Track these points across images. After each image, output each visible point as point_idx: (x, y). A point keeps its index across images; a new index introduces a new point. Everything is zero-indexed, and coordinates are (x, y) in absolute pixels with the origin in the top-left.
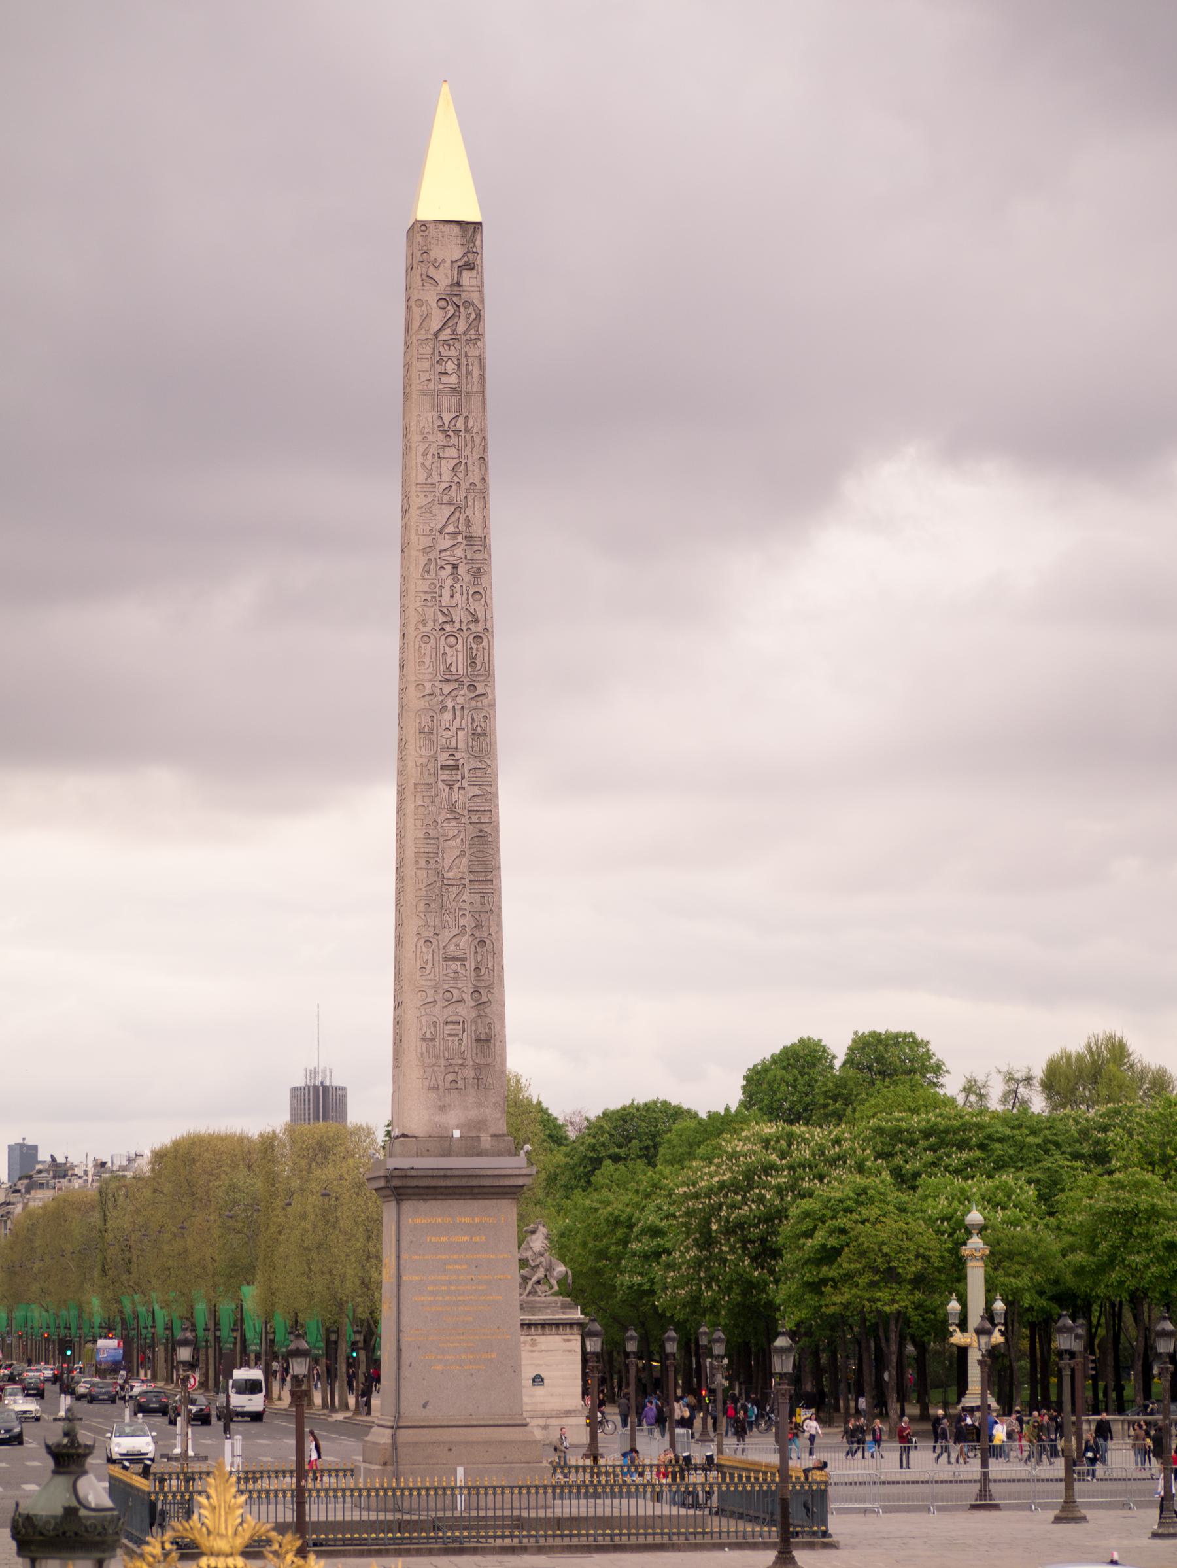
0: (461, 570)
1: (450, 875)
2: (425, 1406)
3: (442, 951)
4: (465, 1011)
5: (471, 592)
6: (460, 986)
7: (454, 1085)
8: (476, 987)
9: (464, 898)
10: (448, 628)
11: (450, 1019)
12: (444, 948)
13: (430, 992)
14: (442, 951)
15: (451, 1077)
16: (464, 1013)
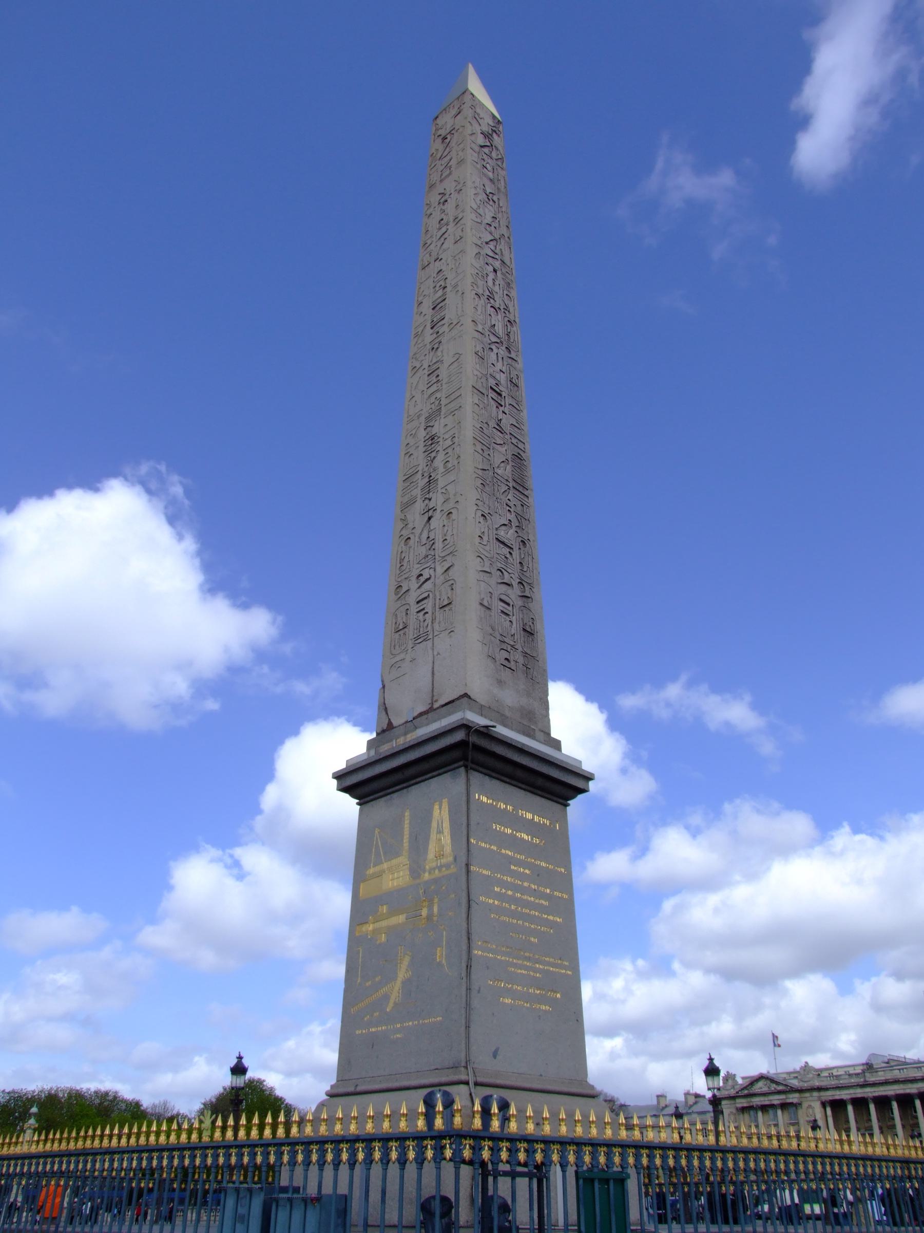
0: (499, 273)
1: (499, 472)
2: (495, 1055)
3: (495, 532)
4: (513, 594)
5: (505, 292)
6: (510, 571)
7: (506, 663)
8: (521, 579)
9: (509, 497)
10: (492, 301)
11: (504, 597)
12: (497, 529)
13: (487, 563)
14: (495, 532)
15: (506, 655)
16: (513, 597)
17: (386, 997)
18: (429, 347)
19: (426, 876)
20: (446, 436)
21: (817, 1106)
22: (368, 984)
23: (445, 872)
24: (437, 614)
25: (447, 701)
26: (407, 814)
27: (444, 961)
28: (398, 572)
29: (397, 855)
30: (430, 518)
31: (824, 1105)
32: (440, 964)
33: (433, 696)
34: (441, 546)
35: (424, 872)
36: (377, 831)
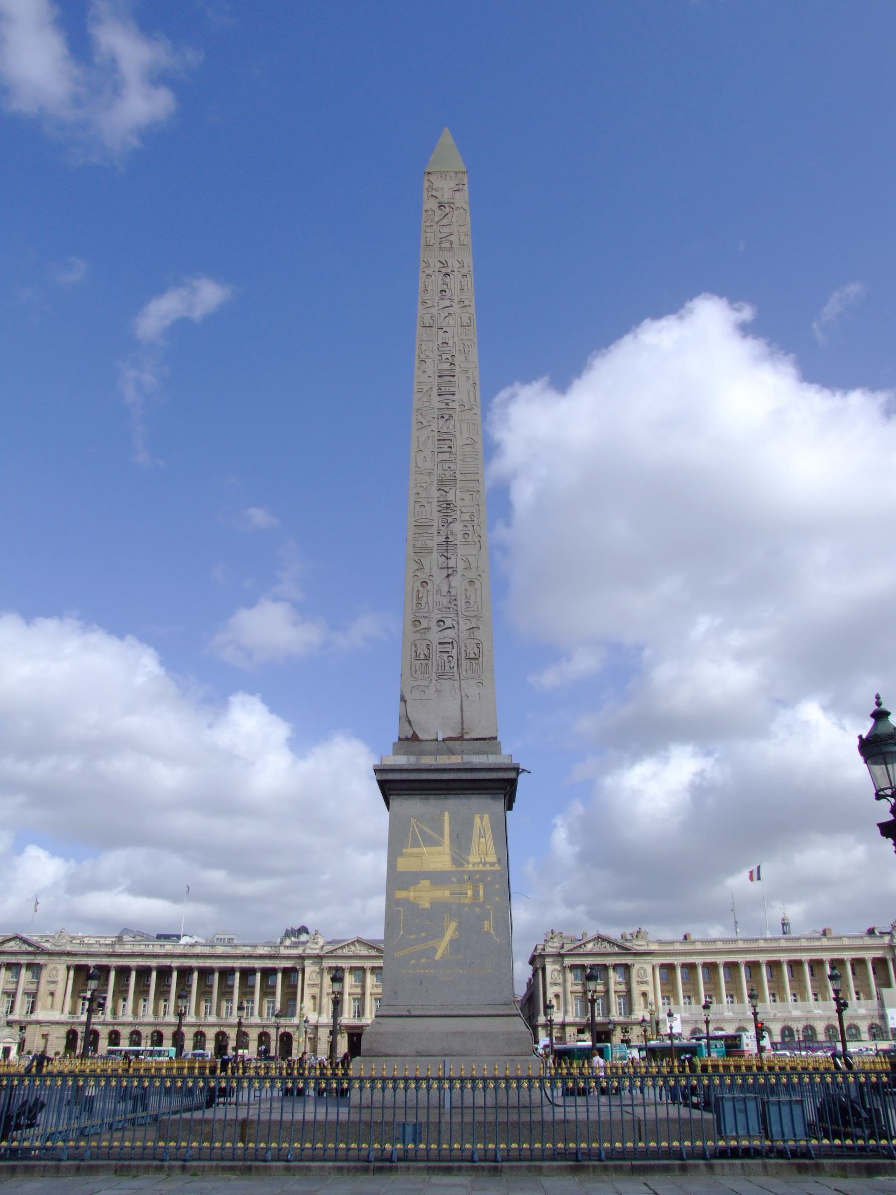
17: (435, 950)
18: (436, 413)
19: (470, 867)
20: (464, 510)
21: (62, 969)
22: (413, 937)
23: (488, 868)
24: (464, 662)
25: (479, 737)
26: (447, 814)
27: (492, 931)
28: (415, 607)
29: (438, 844)
30: (448, 576)
31: (68, 968)
32: (488, 932)
33: (463, 729)
34: (464, 606)
35: (468, 863)
36: (413, 821)
